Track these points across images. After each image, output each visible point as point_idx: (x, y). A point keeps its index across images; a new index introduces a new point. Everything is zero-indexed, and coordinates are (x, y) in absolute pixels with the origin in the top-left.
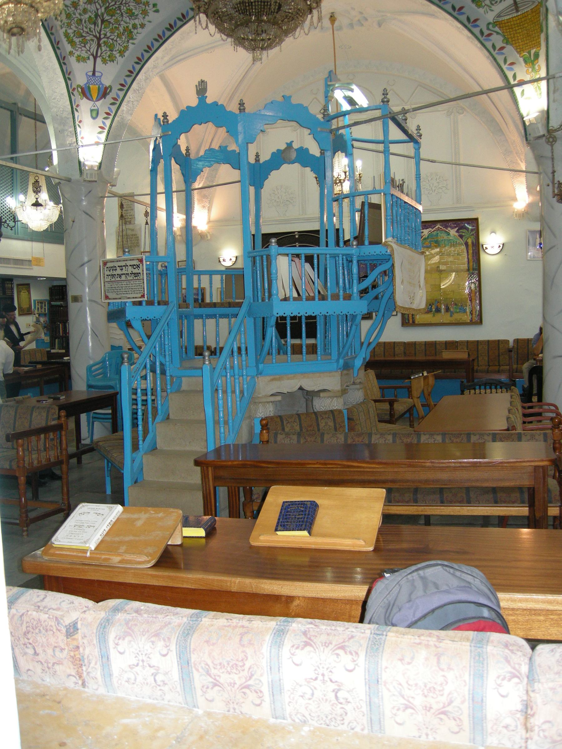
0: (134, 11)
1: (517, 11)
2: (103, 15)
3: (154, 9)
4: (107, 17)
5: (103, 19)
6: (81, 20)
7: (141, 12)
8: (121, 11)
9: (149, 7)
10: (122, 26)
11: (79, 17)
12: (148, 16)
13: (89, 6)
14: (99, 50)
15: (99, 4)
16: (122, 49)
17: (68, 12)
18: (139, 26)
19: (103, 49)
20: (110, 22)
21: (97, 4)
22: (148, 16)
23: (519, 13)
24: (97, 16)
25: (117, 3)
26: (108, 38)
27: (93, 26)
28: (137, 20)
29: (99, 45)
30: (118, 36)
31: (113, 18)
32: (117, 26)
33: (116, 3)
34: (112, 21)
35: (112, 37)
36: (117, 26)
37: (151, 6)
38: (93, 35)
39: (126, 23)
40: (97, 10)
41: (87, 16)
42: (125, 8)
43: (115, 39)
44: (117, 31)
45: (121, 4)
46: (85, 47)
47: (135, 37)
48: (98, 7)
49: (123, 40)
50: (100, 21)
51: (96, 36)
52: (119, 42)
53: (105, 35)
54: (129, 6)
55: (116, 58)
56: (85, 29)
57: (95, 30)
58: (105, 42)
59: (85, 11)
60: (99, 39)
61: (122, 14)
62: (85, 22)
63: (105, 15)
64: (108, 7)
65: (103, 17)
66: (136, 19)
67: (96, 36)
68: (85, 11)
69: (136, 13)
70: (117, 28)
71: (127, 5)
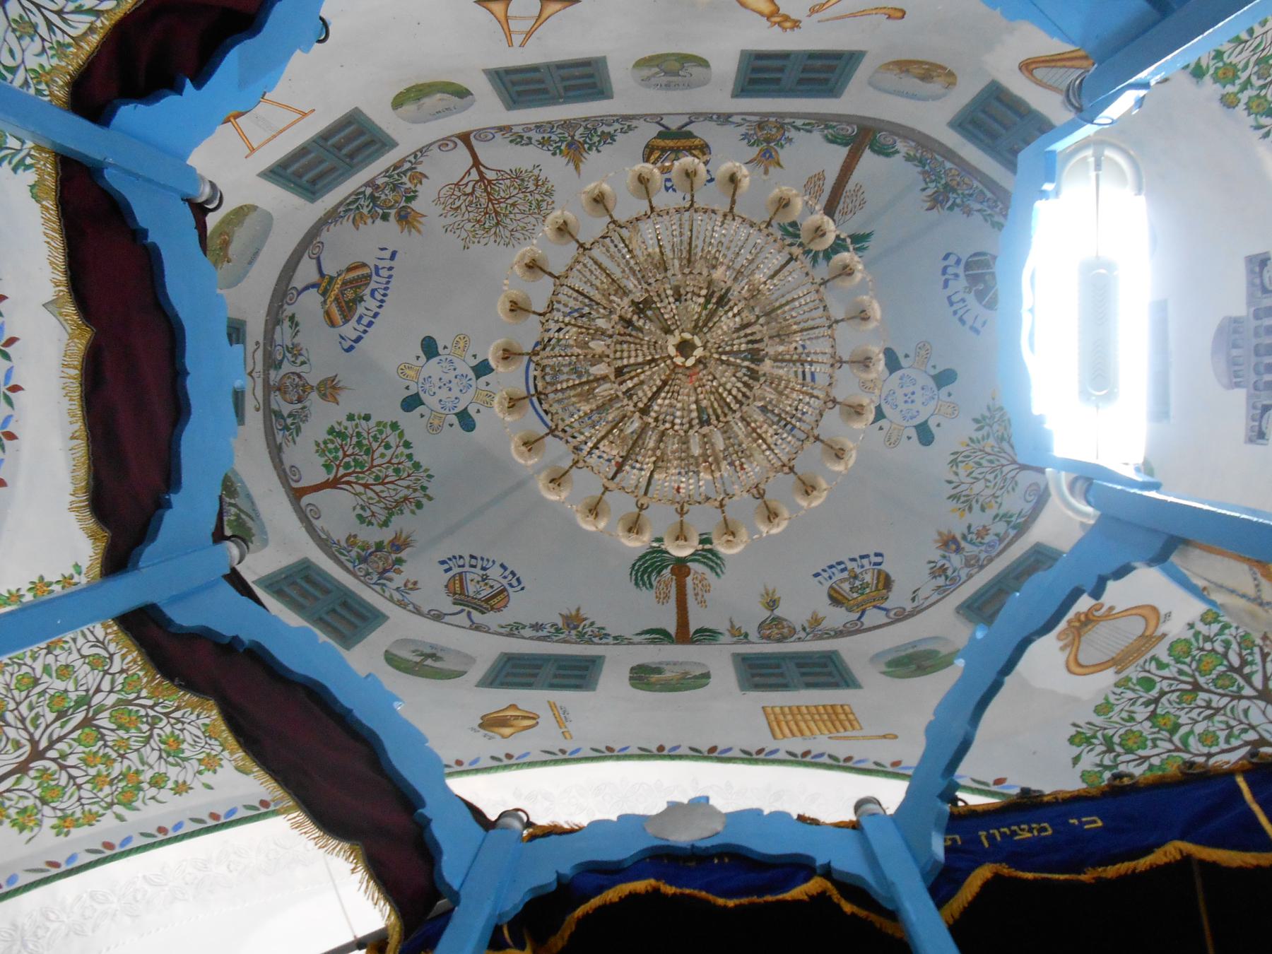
0: (184, 746)
2: (101, 709)
4: (104, 721)
5: (93, 718)
6: (36, 682)
8: (152, 729)
10: (126, 762)
11: (39, 672)
12: (215, 772)
13: (87, 668)
14: (12, 780)
15: (113, 682)
16: (78, 814)
18: (170, 784)
19: (27, 783)
20: (103, 737)
21: (108, 677)
22: (215, 772)
24: (84, 701)
25: (157, 708)
26: (63, 767)
27: (50, 716)
28: (178, 769)
29: (22, 769)
30: (94, 780)
31: (121, 733)
32: (114, 755)
33: (156, 704)
34: (110, 737)
35: (74, 772)
36: (114, 755)
38: (31, 735)
39: (143, 763)
40: (98, 690)
41: (59, 685)
42: (168, 729)
43: (79, 781)
44: (102, 767)
45: (167, 715)
47: (138, 804)
48: (106, 686)
49: (101, 795)
50: (79, 717)
51: (34, 743)
52: (84, 793)
53: (64, 756)
54: (182, 730)
55: (39, 824)
56: (24, 709)
57: (48, 726)
58: (46, 769)
59: (65, 671)
60: (37, 754)
61: (151, 736)
62: (44, 692)
63: (106, 714)
64: (130, 702)
65: (97, 713)
66: (177, 764)
67: (34, 743)
68: (65, 671)
69: (187, 754)
70: (108, 761)
71: (179, 726)
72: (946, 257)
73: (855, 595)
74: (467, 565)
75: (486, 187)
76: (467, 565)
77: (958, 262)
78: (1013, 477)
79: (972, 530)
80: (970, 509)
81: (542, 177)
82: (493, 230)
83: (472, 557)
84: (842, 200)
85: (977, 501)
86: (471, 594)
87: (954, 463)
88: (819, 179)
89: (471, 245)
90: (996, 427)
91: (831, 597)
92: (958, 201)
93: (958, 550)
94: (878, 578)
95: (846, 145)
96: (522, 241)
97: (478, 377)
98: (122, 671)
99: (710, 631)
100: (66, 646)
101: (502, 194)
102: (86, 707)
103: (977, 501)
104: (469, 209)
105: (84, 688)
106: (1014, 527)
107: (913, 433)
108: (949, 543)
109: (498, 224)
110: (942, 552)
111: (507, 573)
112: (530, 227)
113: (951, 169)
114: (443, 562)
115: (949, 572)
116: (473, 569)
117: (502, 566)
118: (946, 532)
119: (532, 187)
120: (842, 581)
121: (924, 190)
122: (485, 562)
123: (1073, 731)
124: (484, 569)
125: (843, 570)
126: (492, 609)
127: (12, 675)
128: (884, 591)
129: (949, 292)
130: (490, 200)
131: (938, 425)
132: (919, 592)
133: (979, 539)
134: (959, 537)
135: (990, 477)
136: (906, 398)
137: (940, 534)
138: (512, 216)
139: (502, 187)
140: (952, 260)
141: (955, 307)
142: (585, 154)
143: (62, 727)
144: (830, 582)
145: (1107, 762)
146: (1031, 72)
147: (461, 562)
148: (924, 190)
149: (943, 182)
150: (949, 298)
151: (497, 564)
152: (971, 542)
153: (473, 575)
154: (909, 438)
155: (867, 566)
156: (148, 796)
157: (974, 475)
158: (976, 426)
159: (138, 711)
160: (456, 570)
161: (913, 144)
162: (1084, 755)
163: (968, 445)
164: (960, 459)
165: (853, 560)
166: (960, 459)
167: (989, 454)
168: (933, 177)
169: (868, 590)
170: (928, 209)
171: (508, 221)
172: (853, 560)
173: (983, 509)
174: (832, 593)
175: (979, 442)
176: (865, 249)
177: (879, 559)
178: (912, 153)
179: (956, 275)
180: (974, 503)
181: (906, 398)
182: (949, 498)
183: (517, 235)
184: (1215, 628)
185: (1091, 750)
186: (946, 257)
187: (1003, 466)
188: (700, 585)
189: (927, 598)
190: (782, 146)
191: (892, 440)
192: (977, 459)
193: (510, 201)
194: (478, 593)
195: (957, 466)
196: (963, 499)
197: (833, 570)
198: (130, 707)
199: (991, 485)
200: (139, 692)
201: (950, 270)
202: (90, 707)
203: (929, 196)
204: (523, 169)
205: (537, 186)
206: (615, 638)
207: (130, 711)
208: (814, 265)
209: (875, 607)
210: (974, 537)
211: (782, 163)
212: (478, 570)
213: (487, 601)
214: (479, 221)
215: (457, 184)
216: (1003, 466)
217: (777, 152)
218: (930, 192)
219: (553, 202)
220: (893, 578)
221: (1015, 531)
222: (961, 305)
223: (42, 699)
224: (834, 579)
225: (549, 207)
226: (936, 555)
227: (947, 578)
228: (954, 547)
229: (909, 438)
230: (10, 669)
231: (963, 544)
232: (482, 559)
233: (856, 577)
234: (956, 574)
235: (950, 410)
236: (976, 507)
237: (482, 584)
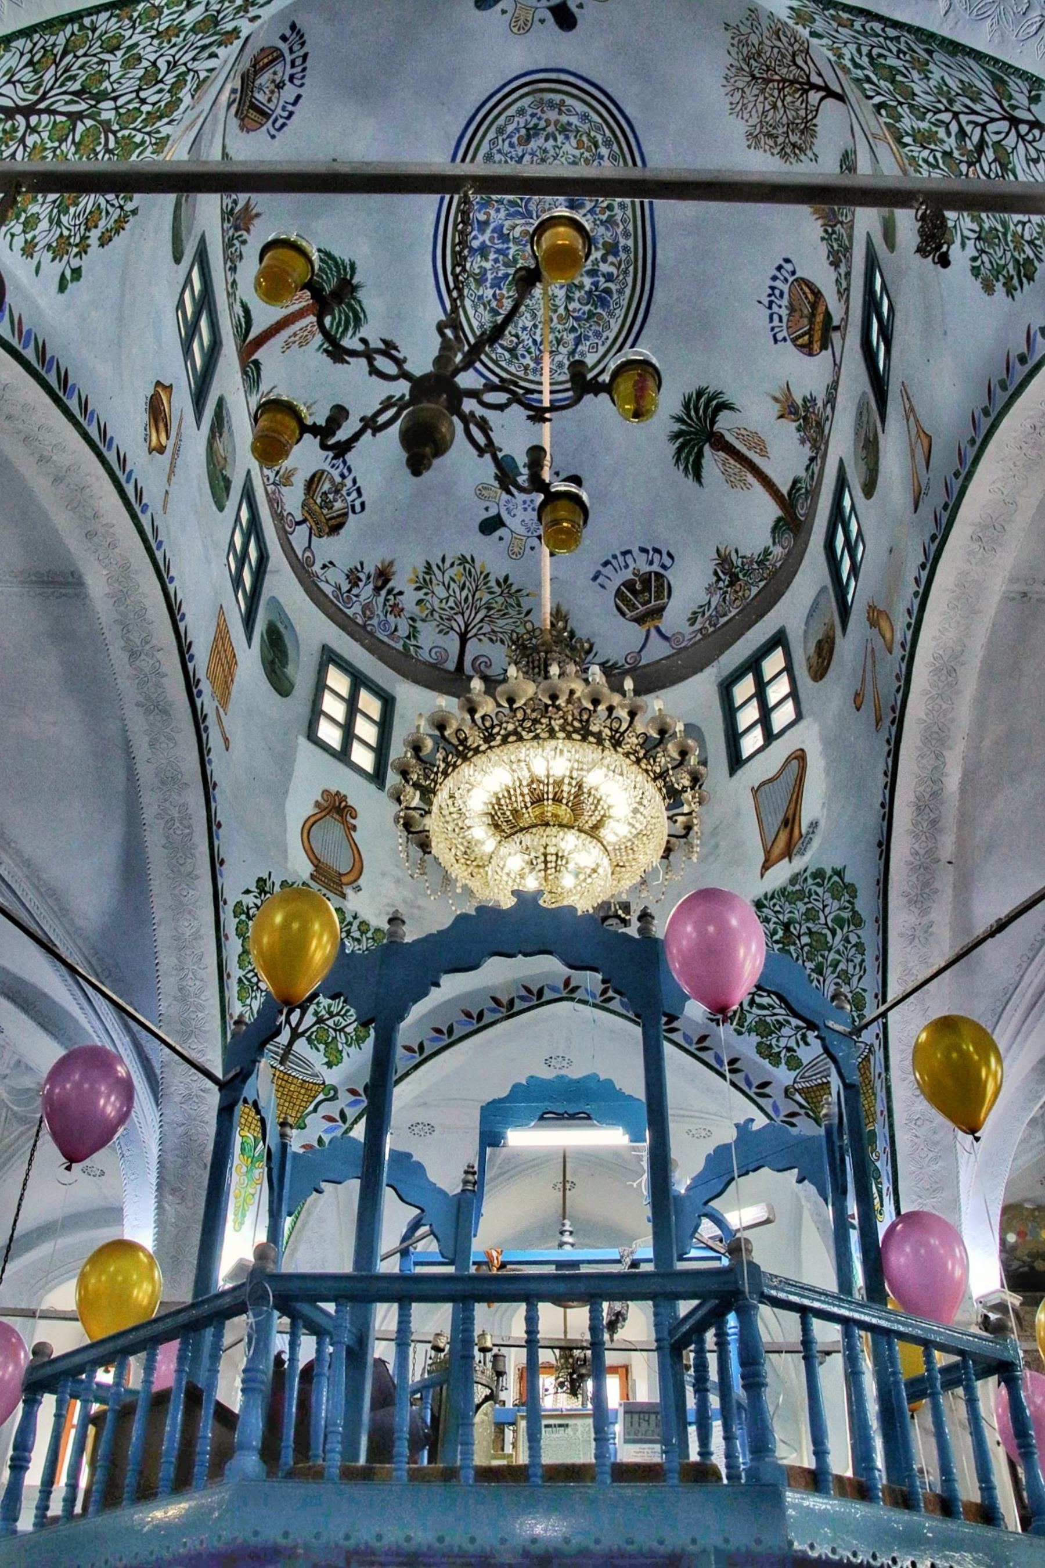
1: (282, 1063)
3: (68, 274)
7: (66, 233)
9: (75, 256)
15: (129, 102)
17: (166, 11)
23: (282, 1068)
27: (76, 86)
37: (75, 263)
40: (115, 99)
46: (30, 63)
53: (34, 130)
57: (65, 93)
62: (102, 62)
63: (89, 123)
65: (89, 117)
68: (132, 60)
69: (64, 219)
72: (670, 555)
73: (319, 501)
74: (294, 56)
75: (800, 83)
76: (294, 56)
77: (664, 567)
78: (452, 629)
79: (399, 597)
80: (418, 589)
81: (802, 157)
82: (747, 69)
83: (305, 57)
84: (739, 466)
85: (426, 594)
86: (257, 82)
87: (463, 560)
88: (761, 450)
89: (729, 34)
90: (500, 600)
91: (314, 476)
92: (721, 584)
93: (377, 590)
94: (338, 516)
95: (790, 493)
96: (729, 99)
97: (551, 9)
98: (143, 101)
99: (259, 375)
100: (165, 44)
101: (789, 99)
102: (93, 103)
103: (426, 594)
104: (776, 50)
105: (116, 86)
106: (405, 646)
107: (493, 512)
108: (383, 576)
109: (753, 77)
110: (373, 572)
111: (290, 108)
112: (746, 116)
113: (750, 590)
114: (293, 27)
115: (355, 591)
116: (288, 66)
117: (299, 97)
118: (394, 569)
119: (794, 138)
120: (332, 480)
121: (737, 552)
122: (299, 76)
123: (265, 876)
124: (292, 78)
125: (343, 476)
126: (242, 119)
127: (120, 28)
128: (327, 530)
129: (636, 551)
130: (784, 80)
131: (501, 539)
132: (332, 569)
133: (390, 609)
134: (388, 586)
135: (451, 603)
136: (528, 503)
137: (391, 564)
138: (761, 98)
139: (798, 103)
140: (667, 561)
141: (621, 558)
142: (820, 222)
143: (67, 103)
144: (328, 468)
145: (251, 912)
146: (795, 758)
147: (296, 47)
148: (737, 552)
149: (741, 576)
150: (629, 552)
151: (300, 91)
152: (387, 600)
153: (283, 71)
154: (487, 509)
155: (350, 499)
156: (12, 231)
157: (452, 583)
158: (501, 581)
159: (100, 143)
160: (284, 47)
161: (778, 565)
162: (252, 895)
163: (481, 573)
164: (467, 566)
165: (354, 481)
166: (467, 566)
167: (473, 596)
168: (746, 567)
169: (325, 511)
170: (718, 550)
171: (755, 92)
172: (354, 481)
173: (420, 602)
174: (318, 475)
175: (485, 584)
176: (686, 475)
177: (358, 508)
178: (770, 557)
179: (651, 563)
180: (424, 591)
181: (528, 503)
182: (428, 563)
183: (738, 95)
184: (357, 935)
185: (256, 897)
186: (670, 555)
187: (463, 614)
188: (306, 333)
189: (327, 582)
190: (799, 430)
191: (484, 492)
192: (468, 583)
193: (779, 104)
194: (260, 89)
195: (460, 564)
196: (427, 577)
197: (342, 466)
198: (102, 136)
199: (443, 605)
200: (121, 129)
201: (657, 556)
202: (95, 106)
203: (730, 554)
204: (815, 140)
205: (794, 145)
206: (234, 282)
207: (99, 138)
208: (673, 417)
209: (311, 529)
210: (391, 603)
211: (782, 420)
212: (289, 71)
213: (254, 107)
214: (759, 53)
215: (807, 53)
216: (463, 614)
217: (795, 421)
218: (734, 557)
219: (772, 154)
220: (342, 531)
221: (401, 648)
222: (623, 564)
223: (95, 66)
224: (332, 471)
225: (767, 147)
226: (370, 568)
227: (349, 591)
228: (380, 583)
229: (487, 509)
230: (127, 21)
231: (384, 592)
232: (304, 70)
233: (337, 491)
234: (354, 599)
235: (516, 550)
236: (420, 594)
237: (272, 87)
